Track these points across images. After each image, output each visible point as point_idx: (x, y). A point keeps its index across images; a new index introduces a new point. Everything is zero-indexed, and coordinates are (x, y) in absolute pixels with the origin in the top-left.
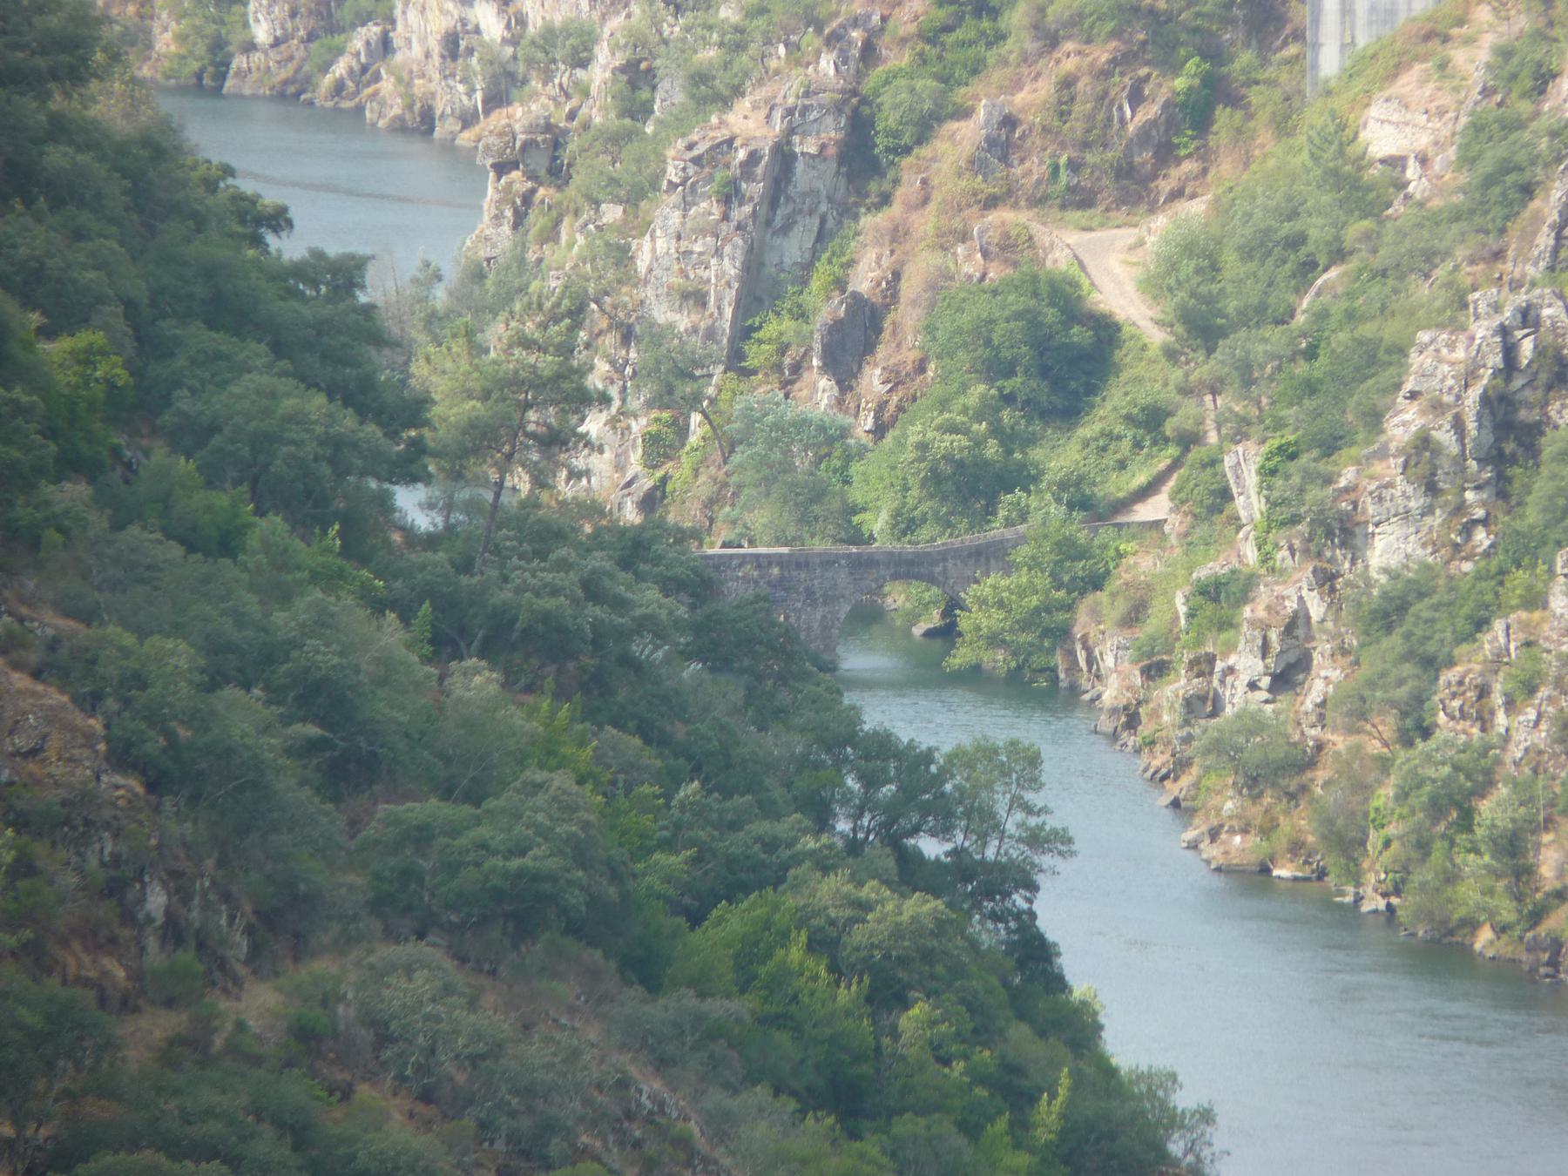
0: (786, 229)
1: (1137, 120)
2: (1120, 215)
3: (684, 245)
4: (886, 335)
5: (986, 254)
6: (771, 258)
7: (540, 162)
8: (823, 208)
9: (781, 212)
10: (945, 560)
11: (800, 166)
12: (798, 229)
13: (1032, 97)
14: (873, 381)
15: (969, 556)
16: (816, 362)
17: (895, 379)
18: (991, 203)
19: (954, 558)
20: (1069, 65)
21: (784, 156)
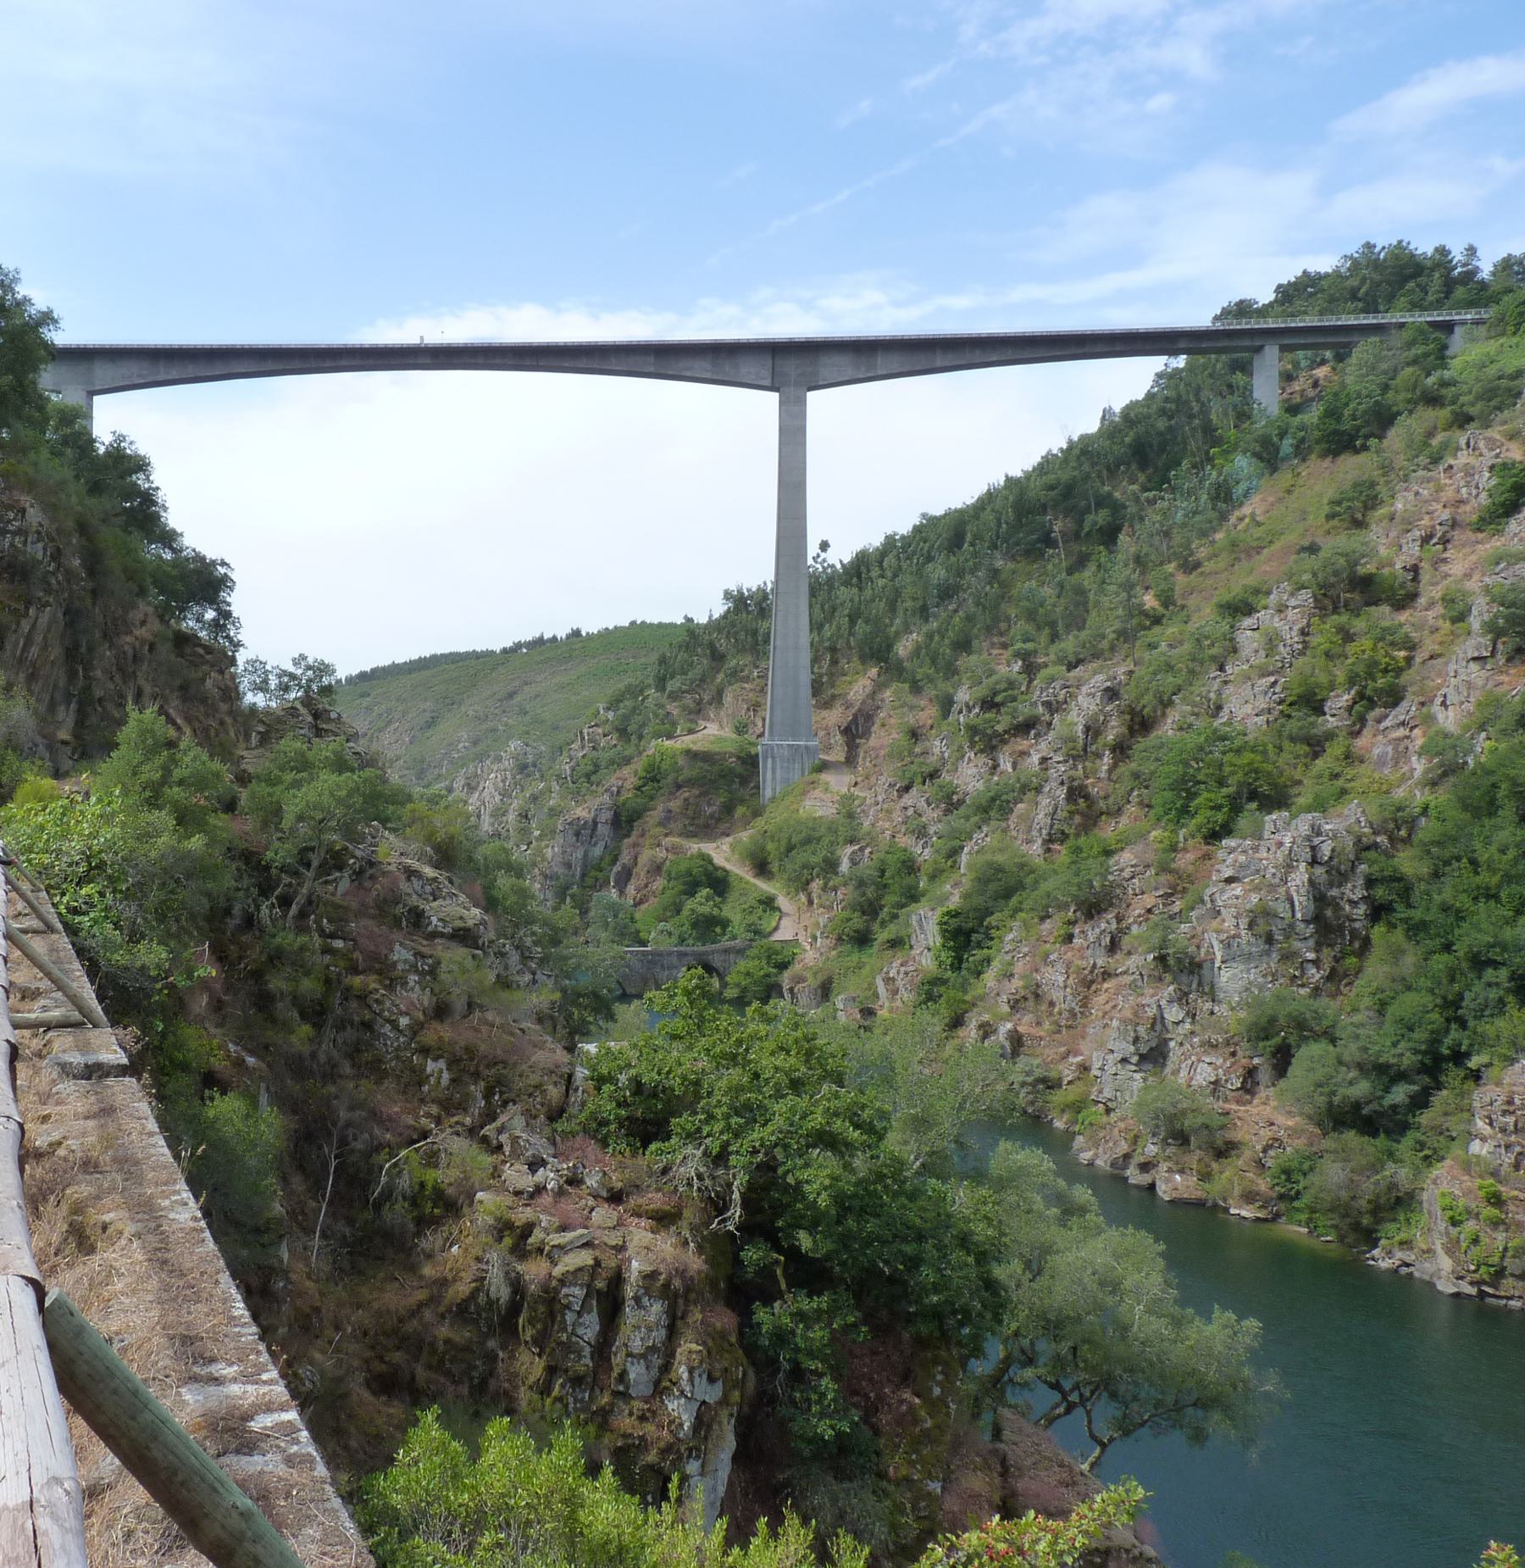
1: (709, 810)
13: (675, 805)
14: (631, 889)
17: (638, 890)
18: (666, 835)
21: (595, 823)
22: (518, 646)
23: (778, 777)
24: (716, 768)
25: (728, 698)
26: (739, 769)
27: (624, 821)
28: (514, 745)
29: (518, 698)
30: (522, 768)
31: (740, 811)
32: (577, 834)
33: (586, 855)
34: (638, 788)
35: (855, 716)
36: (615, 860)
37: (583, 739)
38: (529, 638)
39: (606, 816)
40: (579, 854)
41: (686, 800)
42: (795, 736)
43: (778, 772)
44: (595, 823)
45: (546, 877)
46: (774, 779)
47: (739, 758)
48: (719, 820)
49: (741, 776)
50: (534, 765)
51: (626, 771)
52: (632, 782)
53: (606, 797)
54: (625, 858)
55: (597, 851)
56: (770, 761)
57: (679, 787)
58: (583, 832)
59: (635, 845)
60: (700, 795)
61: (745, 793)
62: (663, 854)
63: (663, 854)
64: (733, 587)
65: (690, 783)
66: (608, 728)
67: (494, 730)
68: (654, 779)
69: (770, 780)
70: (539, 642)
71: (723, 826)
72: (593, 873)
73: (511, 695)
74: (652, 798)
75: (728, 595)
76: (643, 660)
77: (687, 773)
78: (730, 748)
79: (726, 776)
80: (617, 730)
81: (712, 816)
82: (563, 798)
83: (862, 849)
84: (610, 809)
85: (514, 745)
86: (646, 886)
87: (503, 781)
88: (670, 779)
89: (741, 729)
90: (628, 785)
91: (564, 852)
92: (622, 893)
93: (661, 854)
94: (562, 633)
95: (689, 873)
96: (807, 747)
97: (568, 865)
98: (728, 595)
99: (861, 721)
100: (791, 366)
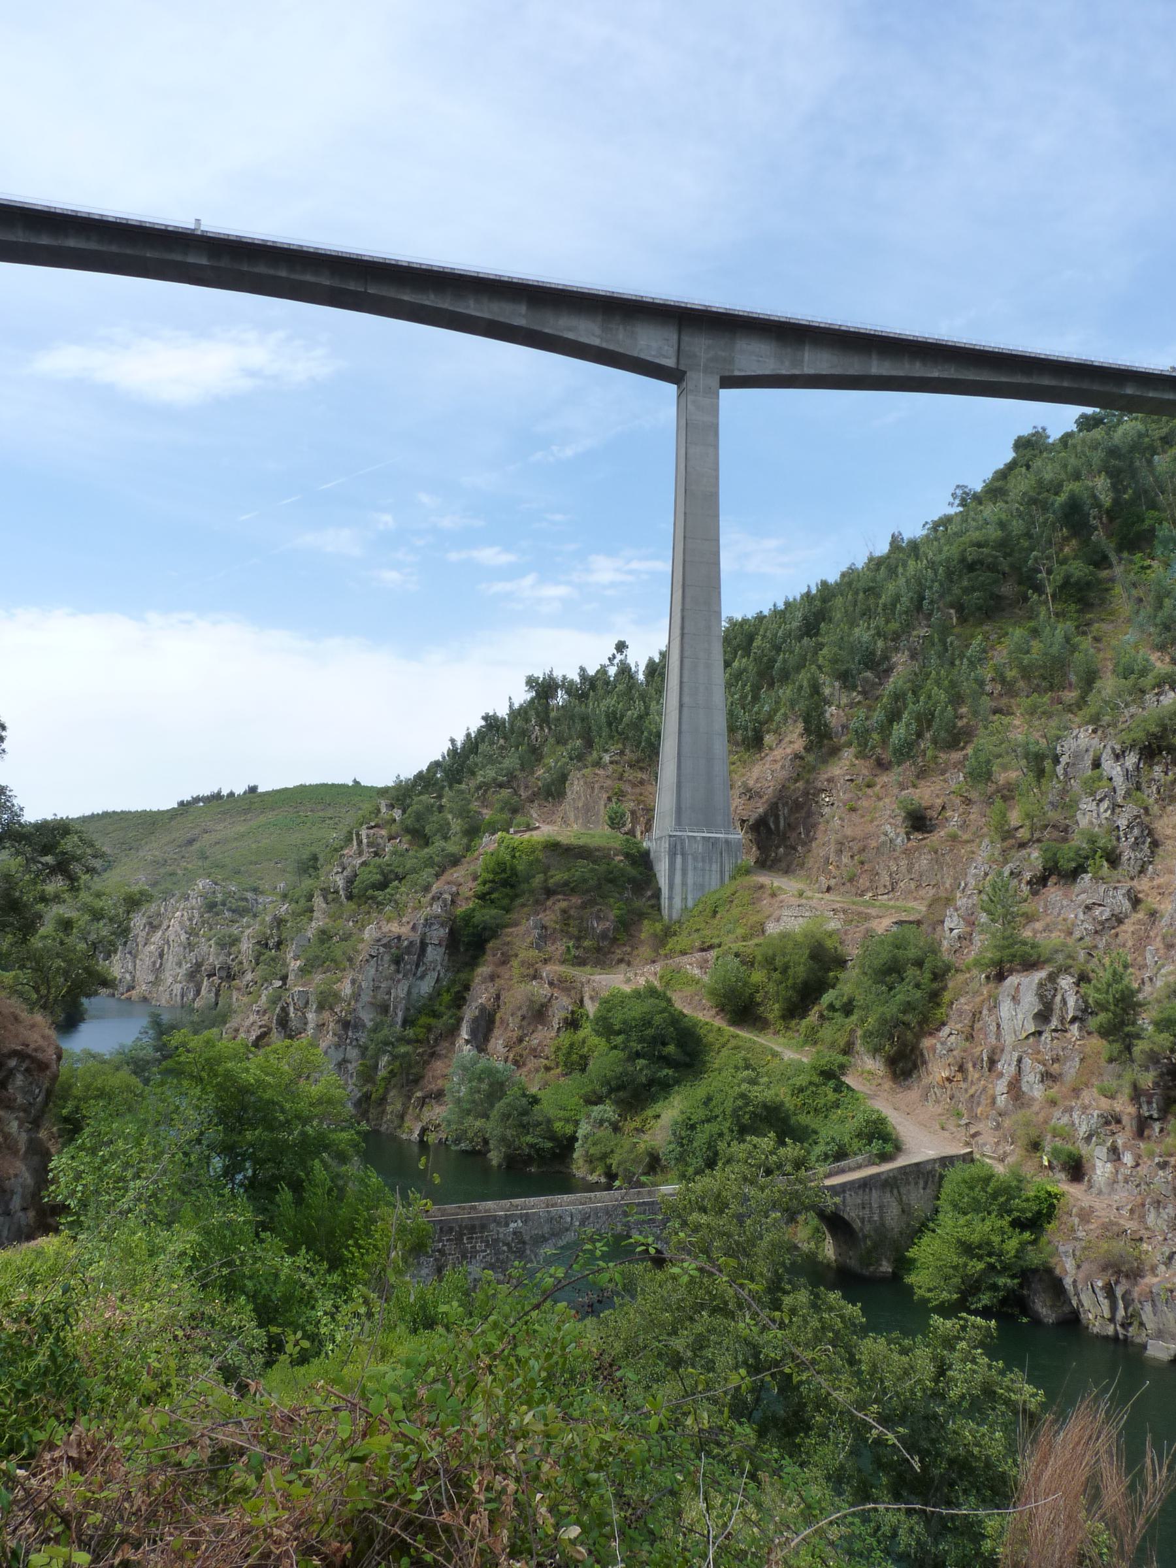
0: (422, 977)
1: (599, 927)
2: (598, 970)
3: (377, 984)
4: (497, 1024)
5: (551, 984)
6: (415, 991)
7: (224, 974)
8: (439, 968)
9: (421, 969)
10: (844, 1192)
11: (429, 949)
12: (428, 977)
13: (550, 917)
14: (497, 1044)
15: (859, 1187)
16: (464, 1034)
18: (546, 961)
19: (850, 1190)
20: (564, 904)
22: (197, 800)
23: (690, 881)
24: (602, 868)
25: (576, 787)
26: (632, 872)
27: (469, 942)
28: (202, 884)
29: (196, 846)
30: (211, 906)
31: (647, 929)
32: (397, 961)
33: (409, 993)
34: (482, 897)
35: (773, 808)
36: (459, 1001)
37: (360, 842)
38: (207, 793)
39: (439, 933)
40: (401, 991)
41: (564, 911)
42: (709, 825)
43: (690, 874)
44: (423, 946)
45: (346, 1025)
46: (684, 884)
47: (627, 855)
48: (614, 940)
49: (632, 880)
50: (224, 904)
51: (457, 874)
52: (469, 888)
53: (437, 909)
54: (481, 996)
55: (426, 987)
56: (679, 859)
57: (549, 892)
58: (403, 957)
59: (492, 978)
60: (584, 906)
61: (640, 903)
62: (546, 990)
63: (546, 990)
64: (539, 674)
65: (568, 888)
66: (394, 828)
67: (173, 874)
68: (505, 883)
69: (674, 884)
70: (217, 797)
71: (619, 953)
72: (424, 1020)
73: (191, 842)
74: (508, 910)
75: (531, 682)
76: (321, 814)
77: (558, 876)
78: (617, 845)
79: (612, 879)
80: (407, 831)
81: (604, 936)
82: (335, 917)
83: (1052, 978)
84: (442, 925)
85: (202, 884)
86: (520, 1040)
87: (190, 920)
88: (538, 880)
89: (615, 822)
90: (466, 891)
91: (376, 989)
92: (481, 1048)
93: (541, 990)
94: (239, 790)
95: (648, 1023)
96: (727, 842)
97: (384, 1009)
98: (531, 682)
99: (784, 812)
100: (701, 346)
